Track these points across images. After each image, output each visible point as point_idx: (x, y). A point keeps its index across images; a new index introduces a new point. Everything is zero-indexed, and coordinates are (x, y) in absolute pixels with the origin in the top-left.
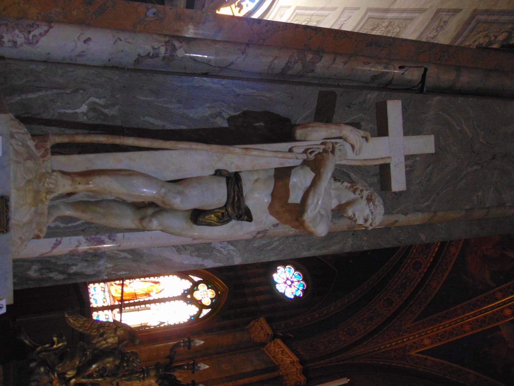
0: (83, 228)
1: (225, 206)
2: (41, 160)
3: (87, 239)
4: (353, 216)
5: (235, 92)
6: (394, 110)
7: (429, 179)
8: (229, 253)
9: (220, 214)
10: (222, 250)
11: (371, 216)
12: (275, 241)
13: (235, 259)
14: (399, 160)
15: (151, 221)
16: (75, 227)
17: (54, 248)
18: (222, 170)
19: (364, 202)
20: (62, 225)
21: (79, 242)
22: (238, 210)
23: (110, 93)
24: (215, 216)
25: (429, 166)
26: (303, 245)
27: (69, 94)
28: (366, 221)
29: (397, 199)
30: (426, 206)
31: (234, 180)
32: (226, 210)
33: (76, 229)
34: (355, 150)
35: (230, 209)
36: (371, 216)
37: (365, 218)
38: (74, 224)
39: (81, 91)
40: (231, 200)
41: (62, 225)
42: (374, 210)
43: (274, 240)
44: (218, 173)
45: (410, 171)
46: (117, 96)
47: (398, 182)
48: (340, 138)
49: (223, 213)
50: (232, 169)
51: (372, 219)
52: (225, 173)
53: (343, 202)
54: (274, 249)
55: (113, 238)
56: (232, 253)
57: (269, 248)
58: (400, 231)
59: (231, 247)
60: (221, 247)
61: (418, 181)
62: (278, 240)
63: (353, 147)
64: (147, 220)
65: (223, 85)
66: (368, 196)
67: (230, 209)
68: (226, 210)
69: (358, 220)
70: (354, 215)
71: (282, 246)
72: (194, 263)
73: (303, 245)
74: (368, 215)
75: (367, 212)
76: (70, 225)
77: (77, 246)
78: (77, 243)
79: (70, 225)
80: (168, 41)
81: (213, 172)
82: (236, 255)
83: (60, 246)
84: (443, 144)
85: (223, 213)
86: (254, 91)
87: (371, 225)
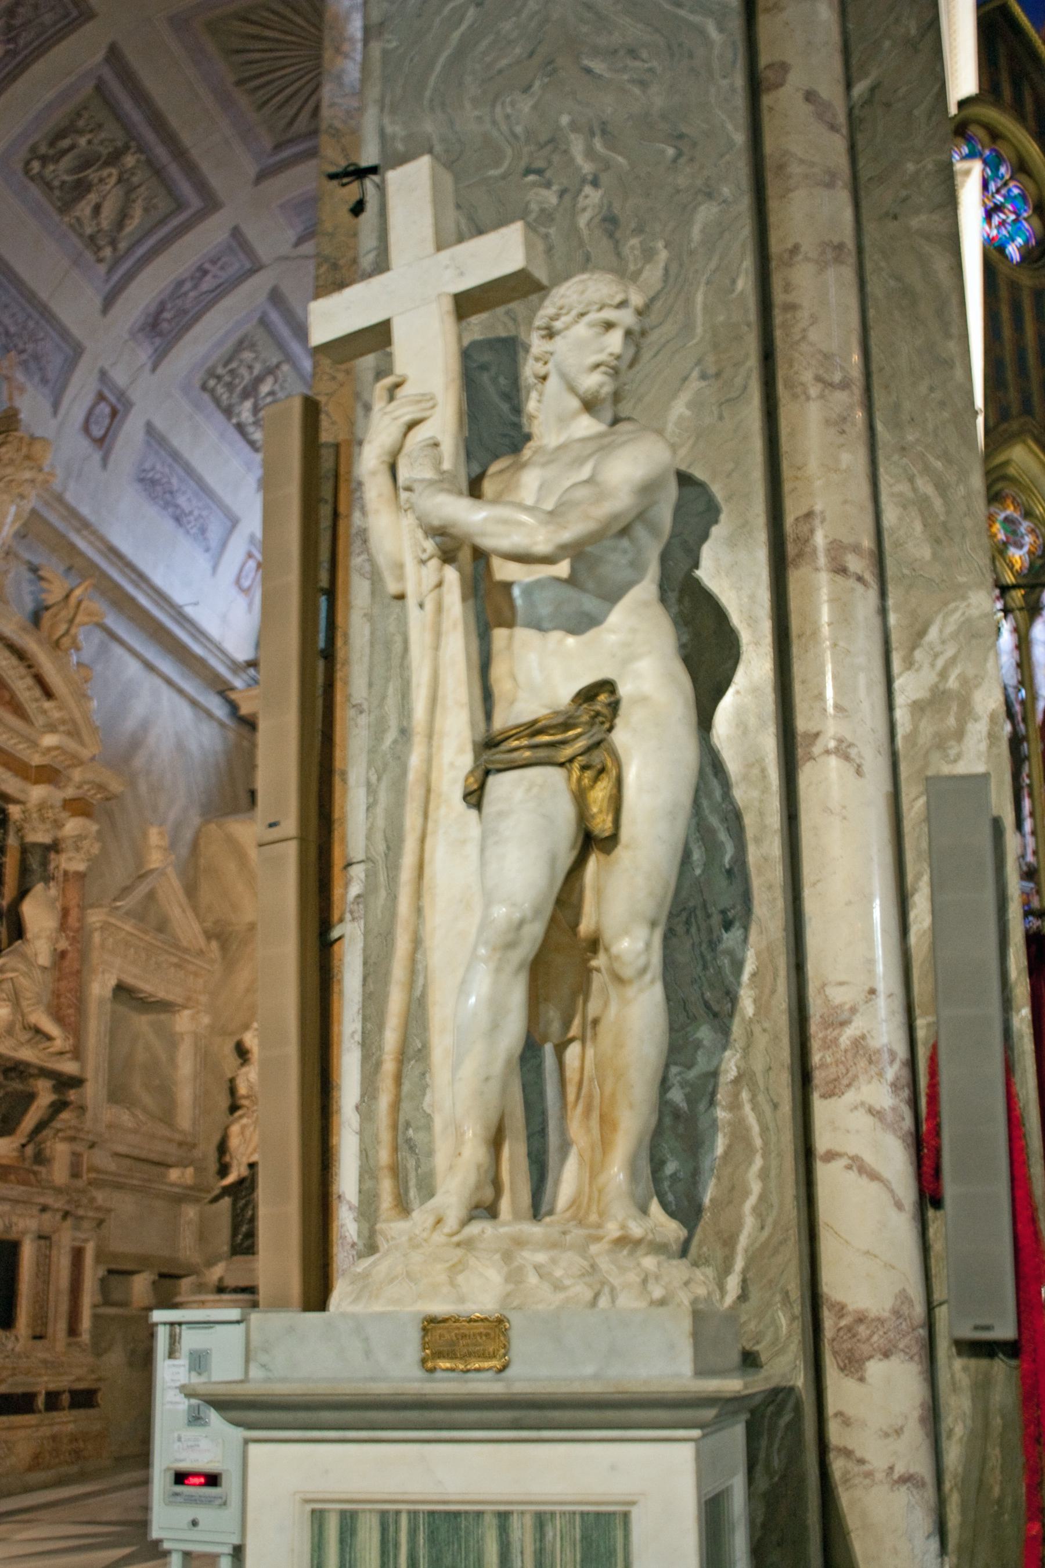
0: (767, 1108)
1: (562, 765)
2: (391, 1243)
3: (849, 1086)
4: (603, 369)
5: (395, 742)
6: (332, 318)
7: (633, 53)
8: (955, 635)
9: (588, 774)
10: (940, 663)
11: (593, 316)
12: (915, 490)
13: (975, 612)
14: (447, 267)
15: (618, 958)
16: (764, 1130)
17: (874, 1176)
18: (466, 787)
19: (559, 344)
20: (758, 1162)
21: (856, 1108)
22: (573, 726)
23: (412, 1062)
24: (592, 787)
25: (588, 71)
26: (932, 389)
27: (418, 1161)
28: (609, 326)
29: (694, 145)
30: (721, 30)
31: (494, 753)
32: (571, 760)
33: (771, 1125)
34: (418, 416)
35: (568, 752)
36: (593, 316)
37: (597, 330)
38: (756, 1129)
39: (411, 1132)
40: (542, 753)
41: (758, 1162)
42: (574, 313)
43: (910, 495)
44: (475, 797)
45: (604, 132)
46: (420, 1046)
47: (501, 252)
48: (393, 469)
49: (584, 768)
50: (466, 761)
51: (601, 309)
52: (471, 780)
53: (575, 403)
54: (942, 488)
55: (845, 1015)
56: (950, 628)
57: (938, 503)
58: (887, 44)
59: (933, 634)
60: (933, 665)
61: (637, 91)
62: (911, 480)
63: (411, 426)
64: (616, 965)
65: (379, 779)
66: (543, 337)
67: (568, 752)
68: (571, 760)
69: (610, 350)
70: (597, 366)
71: (932, 459)
72: (983, 746)
73: (932, 389)
74: (591, 325)
75: (581, 330)
76: (758, 1142)
77: (871, 1111)
78: (862, 1111)
79: (758, 1142)
80: (351, 912)
81: (473, 813)
82: (957, 615)
83: (869, 1158)
84: (518, 50)
85: (584, 768)
86: (391, 691)
87: (622, 304)
